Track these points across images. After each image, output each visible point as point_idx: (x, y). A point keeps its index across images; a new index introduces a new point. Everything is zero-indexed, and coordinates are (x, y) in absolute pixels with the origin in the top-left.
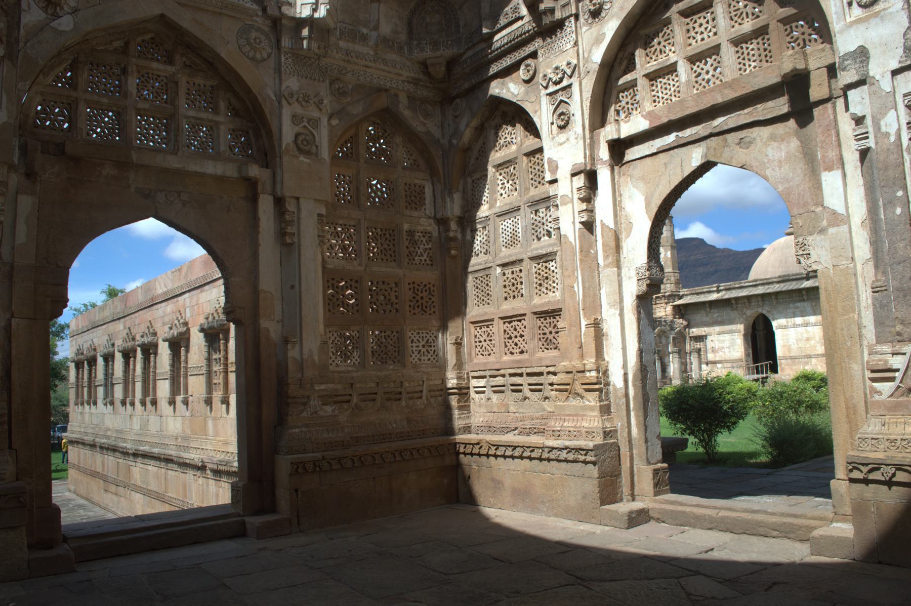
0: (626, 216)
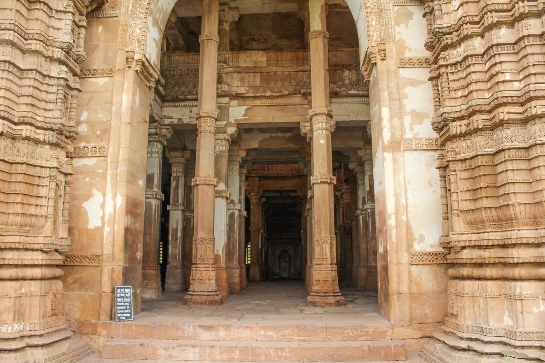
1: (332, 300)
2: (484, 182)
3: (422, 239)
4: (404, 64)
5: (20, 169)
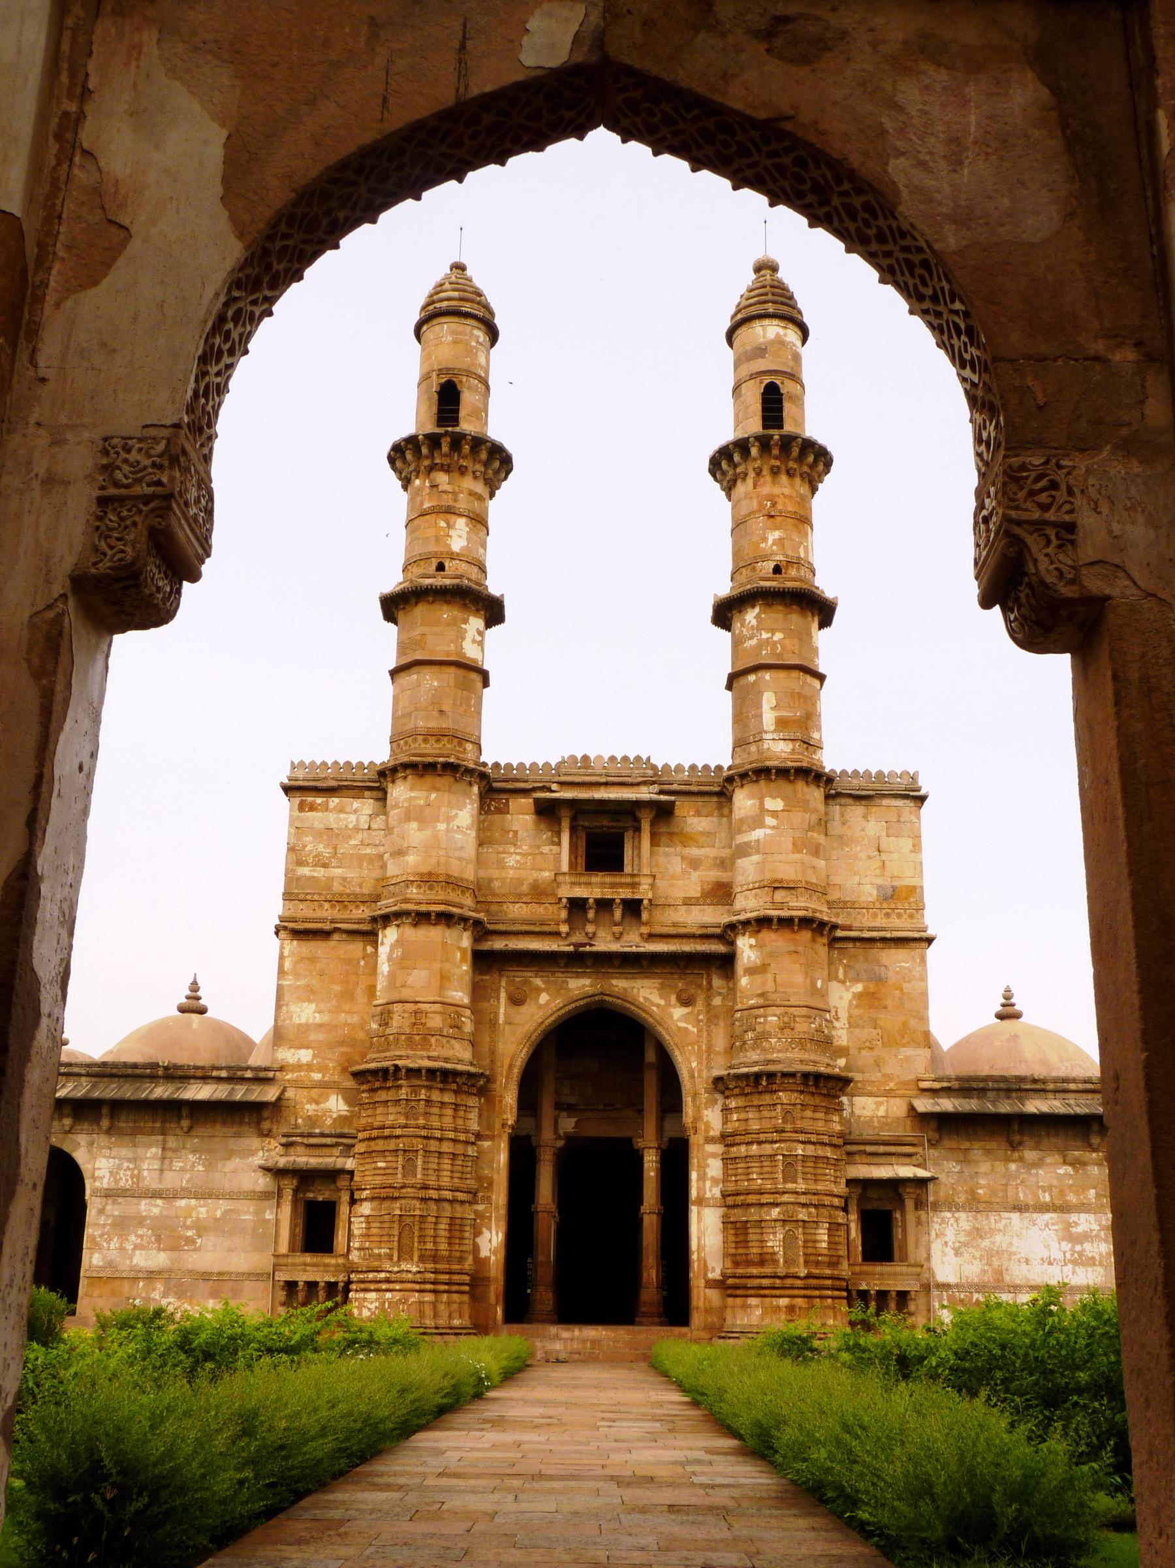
0: (96, 191)
1: (656, 1320)
2: (741, 1238)
3: (713, 1270)
4: (710, 1140)
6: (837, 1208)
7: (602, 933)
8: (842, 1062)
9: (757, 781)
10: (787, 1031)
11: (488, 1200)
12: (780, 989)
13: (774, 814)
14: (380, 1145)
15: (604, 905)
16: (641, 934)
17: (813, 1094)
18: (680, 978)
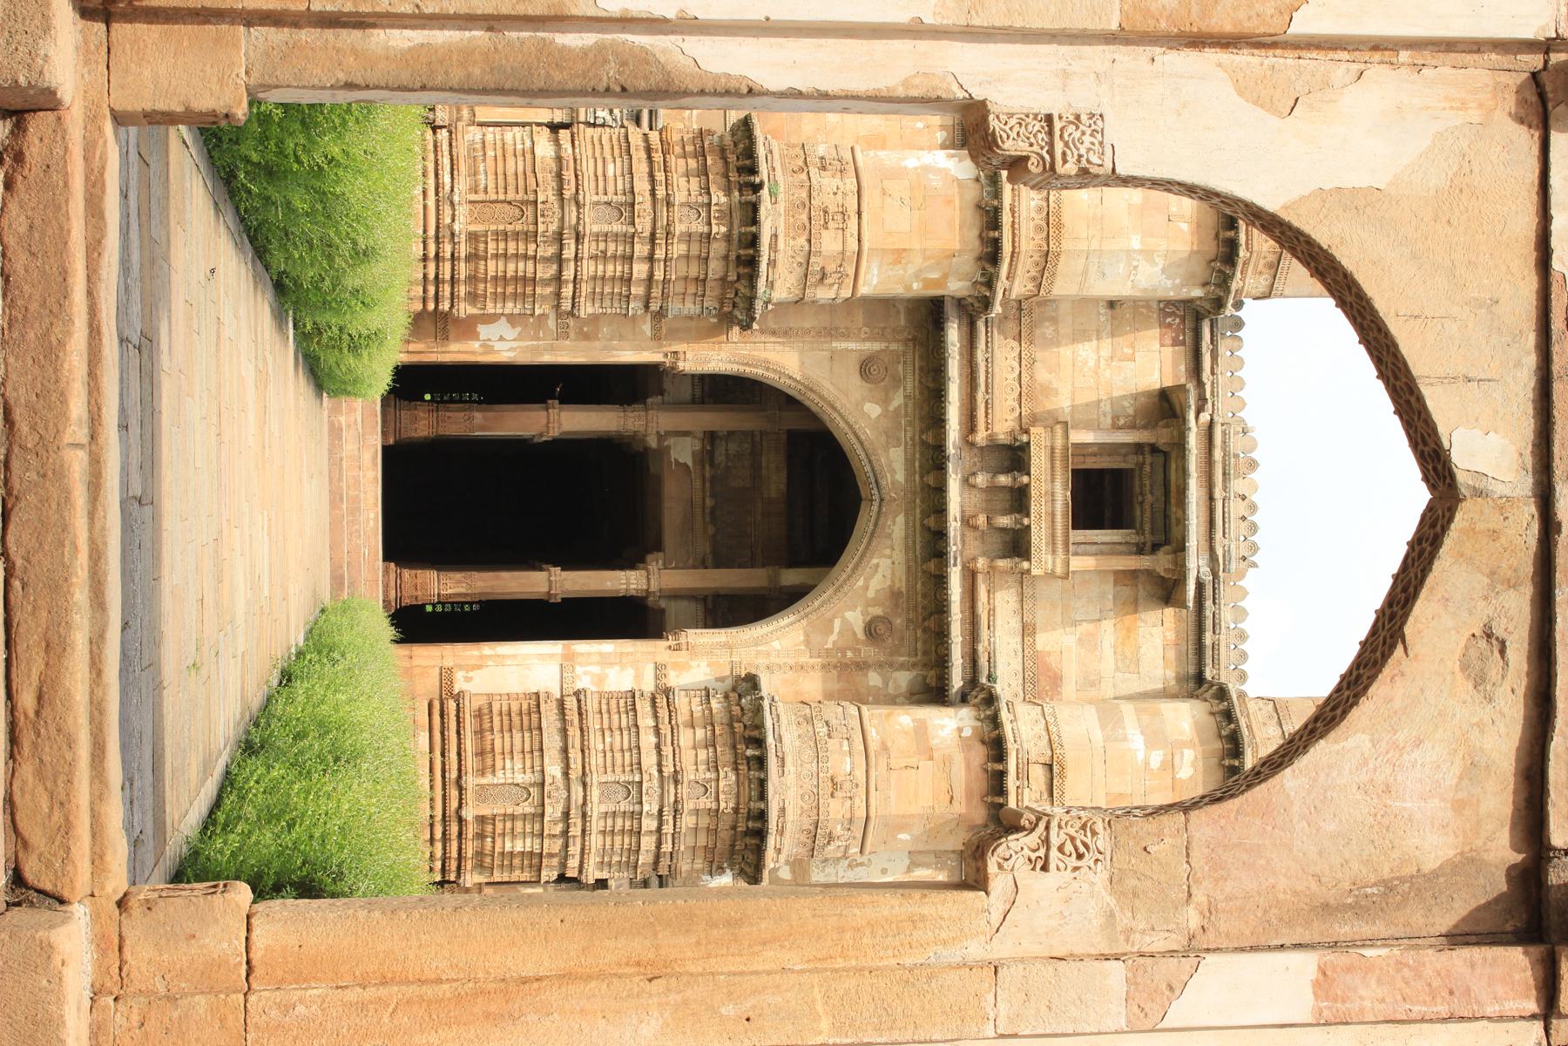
0: (1326, 84)
2: (516, 719)
3: (468, 680)
4: (659, 669)
5: (529, 290)
6: (564, 865)
7: (976, 499)
8: (785, 873)
9: (1220, 736)
10: (826, 788)
11: (563, 334)
12: (894, 774)
13: (1170, 765)
14: (641, 168)
15: (1019, 500)
16: (974, 559)
17: (734, 828)
18: (908, 620)
